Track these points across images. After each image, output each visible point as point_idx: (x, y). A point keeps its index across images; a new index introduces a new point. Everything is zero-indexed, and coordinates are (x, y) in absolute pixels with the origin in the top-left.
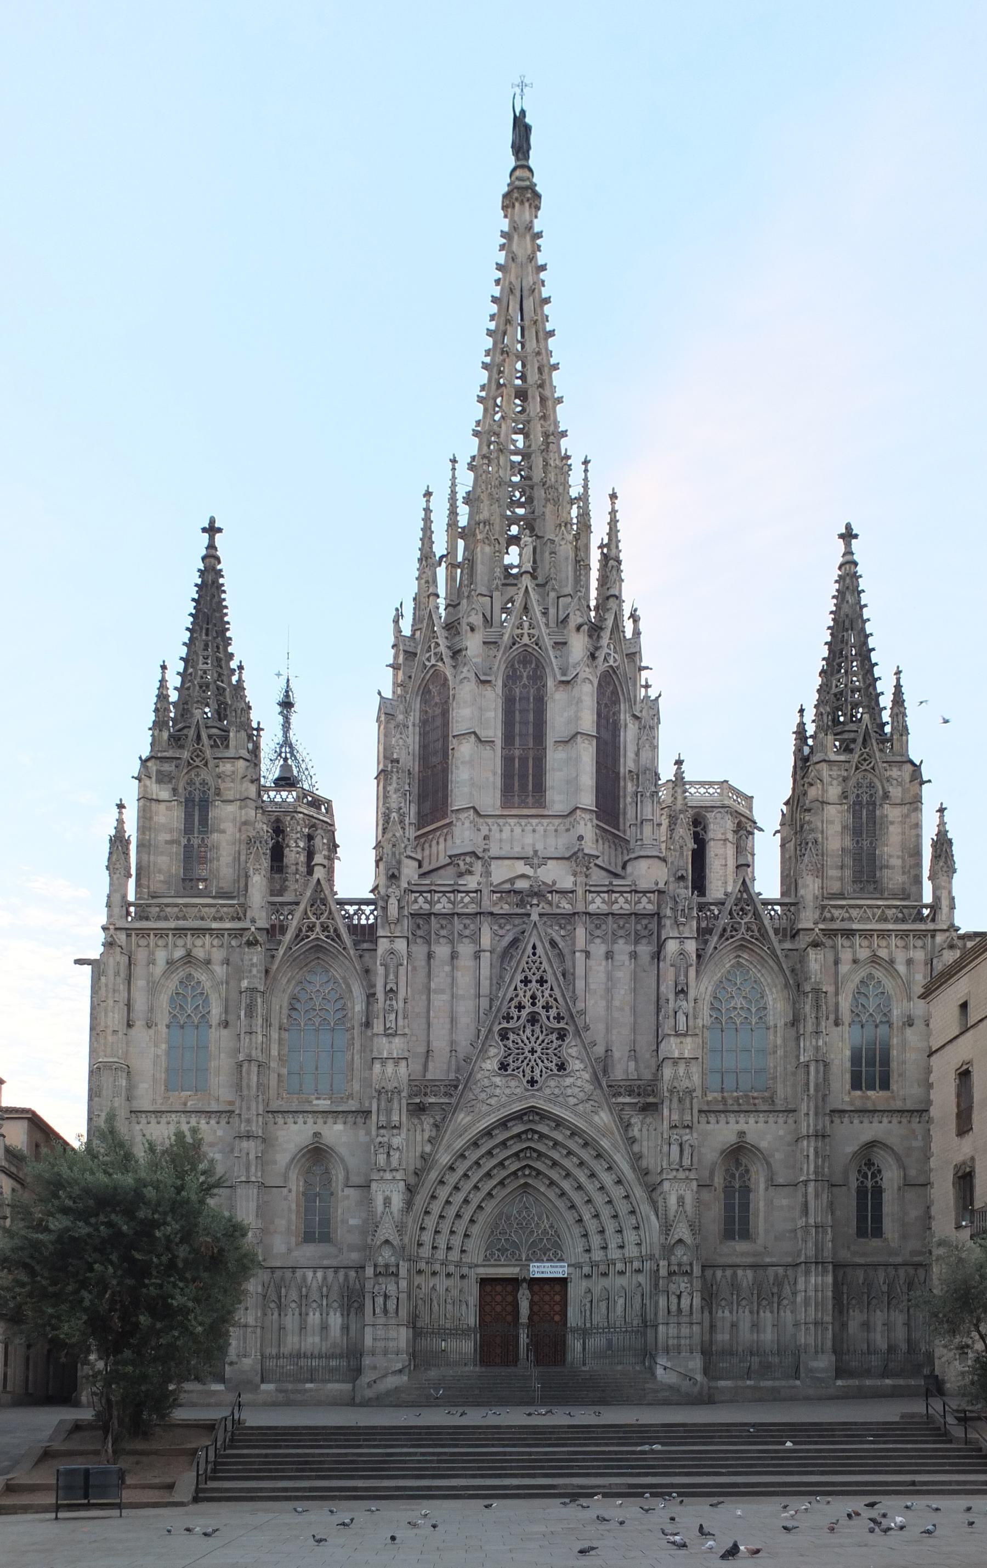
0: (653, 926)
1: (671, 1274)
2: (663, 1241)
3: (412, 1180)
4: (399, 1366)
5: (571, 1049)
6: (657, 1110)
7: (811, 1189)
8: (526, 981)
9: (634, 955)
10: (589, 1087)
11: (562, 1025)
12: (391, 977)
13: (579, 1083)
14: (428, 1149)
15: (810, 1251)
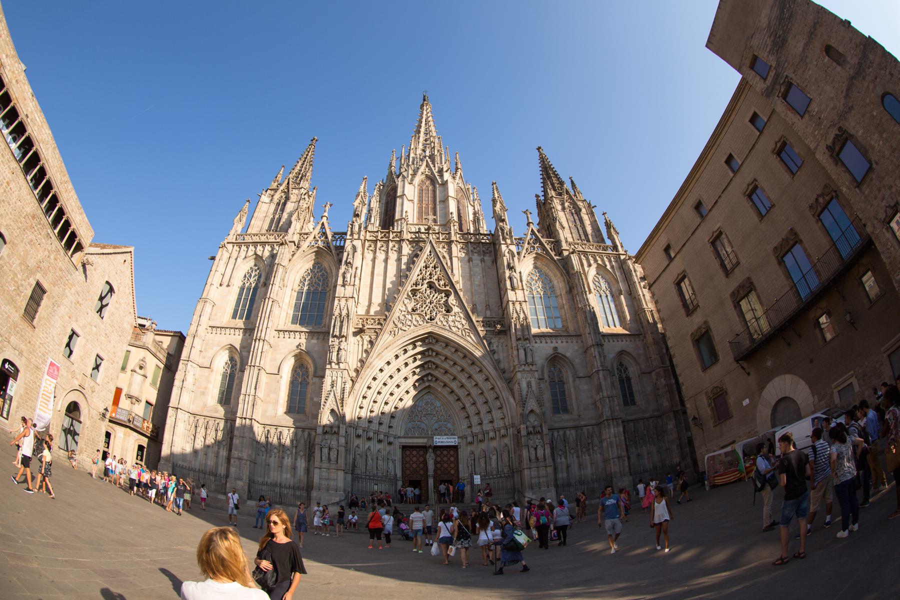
0: (492, 248)
1: (529, 434)
2: (520, 410)
3: (354, 374)
4: (337, 499)
5: (452, 300)
6: (506, 334)
7: (601, 376)
8: (426, 267)
9: (482, 261)
10: (464, 322)
11: (448, 288)
12: (351, 256)
13: (458, 319)
14: (364, 355)
15: (607, 413)
